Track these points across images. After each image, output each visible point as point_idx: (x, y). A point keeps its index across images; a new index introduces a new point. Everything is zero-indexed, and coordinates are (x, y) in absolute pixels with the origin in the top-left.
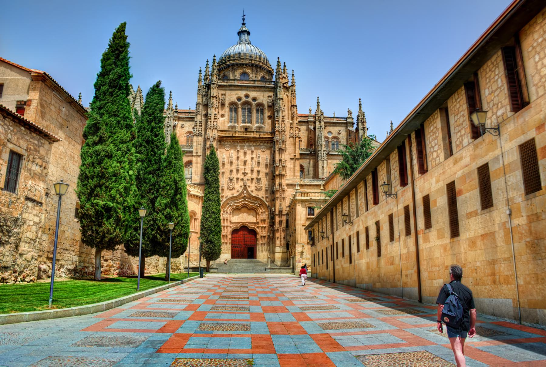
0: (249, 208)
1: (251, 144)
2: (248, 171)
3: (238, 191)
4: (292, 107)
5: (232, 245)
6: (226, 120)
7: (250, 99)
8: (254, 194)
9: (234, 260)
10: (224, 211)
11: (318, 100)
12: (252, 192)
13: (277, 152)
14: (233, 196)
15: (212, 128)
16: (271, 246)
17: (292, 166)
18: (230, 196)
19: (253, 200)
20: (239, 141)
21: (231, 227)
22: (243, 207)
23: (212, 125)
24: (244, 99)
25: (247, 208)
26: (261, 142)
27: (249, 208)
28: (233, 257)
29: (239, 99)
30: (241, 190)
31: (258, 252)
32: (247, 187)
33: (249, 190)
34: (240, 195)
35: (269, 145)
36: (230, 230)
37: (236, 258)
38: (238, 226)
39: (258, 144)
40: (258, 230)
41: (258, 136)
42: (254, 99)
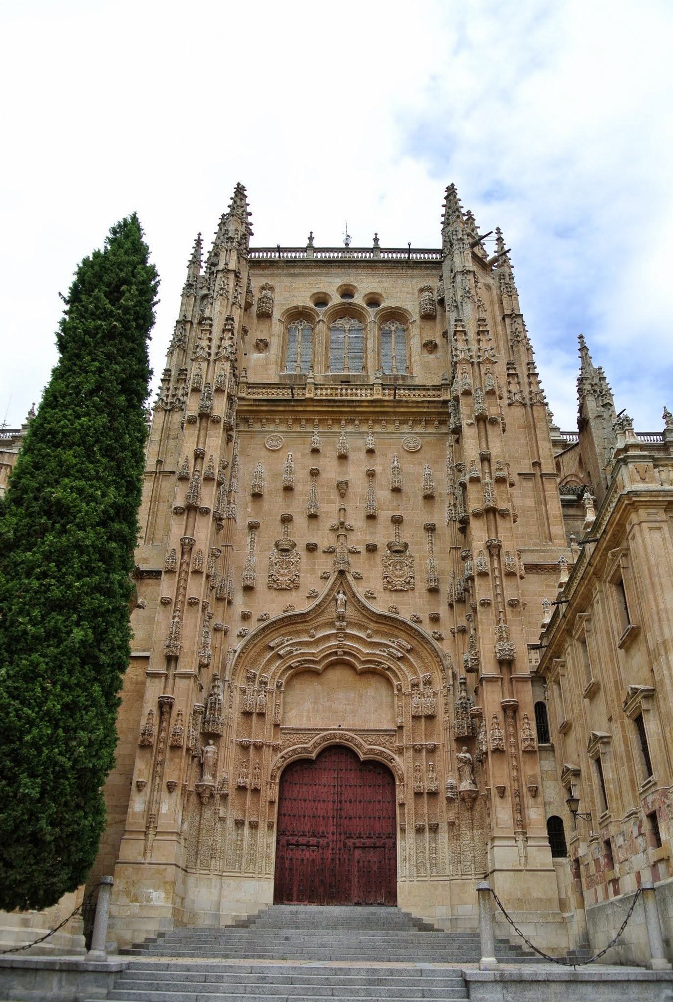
0: (360, 667)
1: (364, 428)
2: (355, 520)
3: (312, 596)
4: (507, 320)
5: (281, 833)
6: (273, 358)
7: (358, 300)
8: (378, 607)
9: (283, 908)
10: (251, 679)
11: (582, 343)
12: (371, 597)
13: (470, 434)
14: (289, 614)
15: (212, 358)
16: (466, 837)
17: (530, 502)
18: (275, 614)
19: (377, 632)
20: (317, 417)
21: (276, 749)
22: (332, 665)
23: (213, 351)
24: (336, 299)
25: (351, 666)
26: (403, 422)
27: (360, 667)
28: (282, 895)
29: (321, 300)
30: (323, 589)
31: (403, 870)
32: (350, 578)
33: (360, 590)
34: (319, 610)
35: (431, 430)
36: (273, 762)
37: (300, 901)
38: (310, 746)
39: (391, 428)
40: (401, 764)
41: (392, 398)
42: (373, 301)
